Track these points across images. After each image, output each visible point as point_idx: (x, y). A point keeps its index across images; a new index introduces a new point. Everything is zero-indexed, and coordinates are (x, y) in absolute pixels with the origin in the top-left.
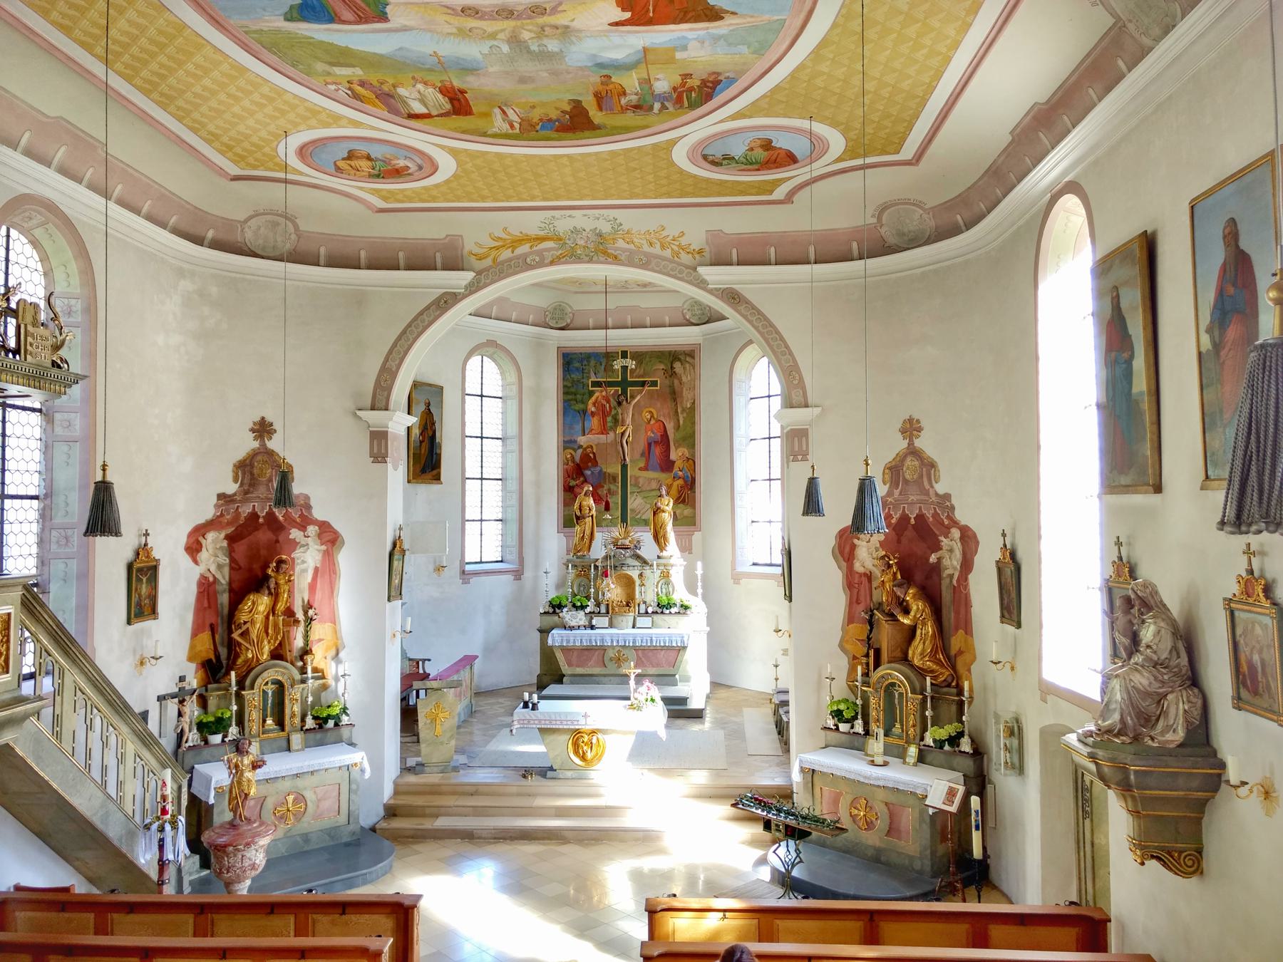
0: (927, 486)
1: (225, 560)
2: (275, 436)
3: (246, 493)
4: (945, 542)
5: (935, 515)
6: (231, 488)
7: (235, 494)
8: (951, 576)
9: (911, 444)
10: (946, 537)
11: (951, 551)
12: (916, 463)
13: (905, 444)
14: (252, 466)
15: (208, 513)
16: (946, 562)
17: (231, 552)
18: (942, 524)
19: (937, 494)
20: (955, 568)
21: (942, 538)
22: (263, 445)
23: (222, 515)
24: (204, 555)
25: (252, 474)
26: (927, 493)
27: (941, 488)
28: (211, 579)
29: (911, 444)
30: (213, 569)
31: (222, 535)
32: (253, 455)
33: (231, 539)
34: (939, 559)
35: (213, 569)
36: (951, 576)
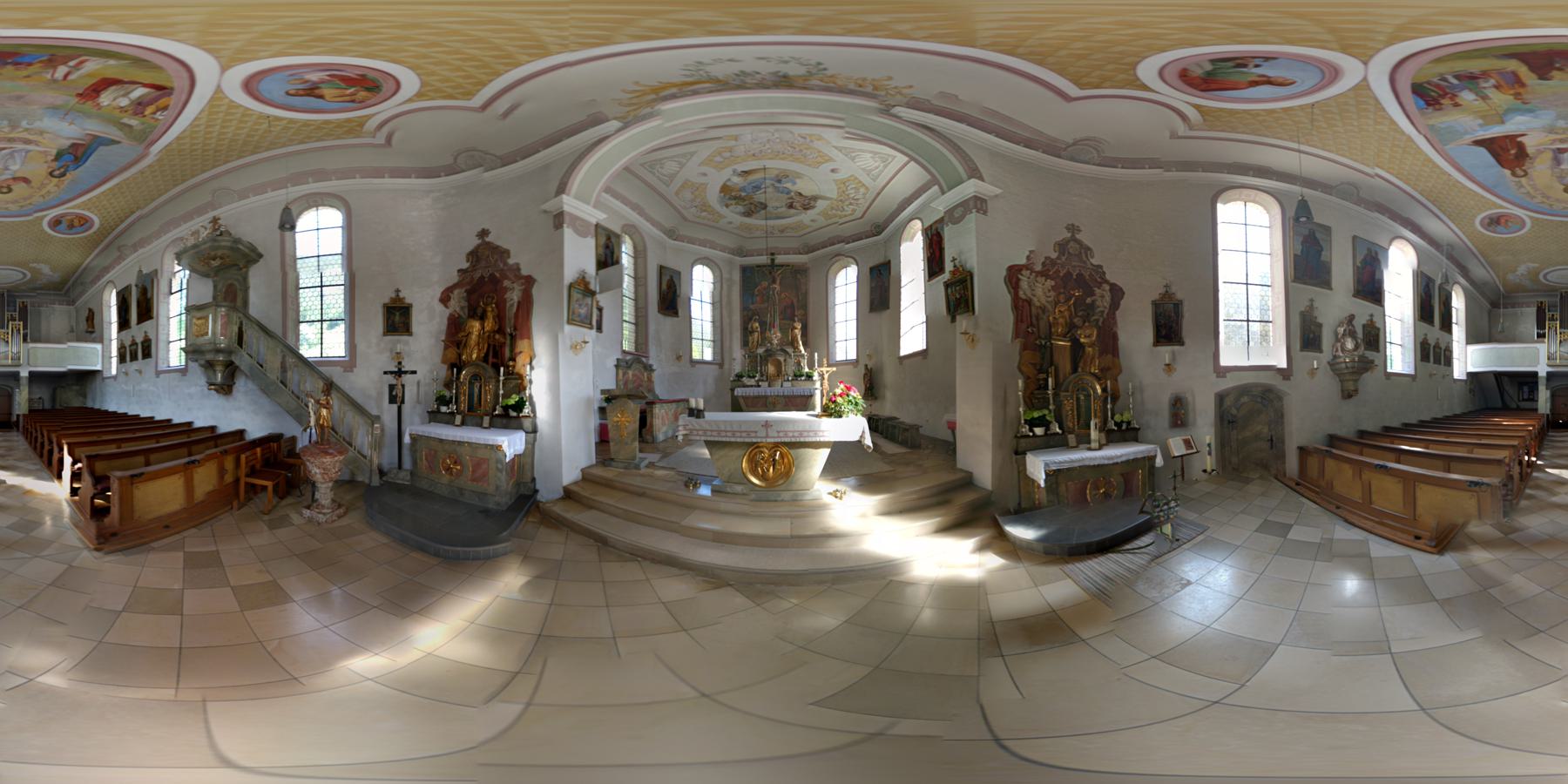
0: (1085, 259)
1: (466, 304)
2: (490, 235)
3: (474, 266)
4: (1098, 291)
5: (1091, 275)
6: (465, 265)
7: (467, 268)
8: (1103, 312)
9: (1073, 235)
10: (1099, 288)
11: (1103, 297)
12: (1078, 246)
13: (1069, 235)
14: (478, 252)
15: (455, 278)
16: (1099, 303)
17: (468, 300)
18: (1096, 280)
19: (1092, 264)
20: (1105, 307)
21: (1096, 289)
22: (483, 240)
23: (463, 279)
24: (452, 303)
25: (477, 256)
26: (1085, 262)
27: (1094, 261)
28: (457, 316)
29: (1073, 235)
30: (458, 309)
31: (463, 290)
32: (478, 246)
33: (469, 292)
34: (1093, 302)
35: (458, 309)
36: (1103, 312)
